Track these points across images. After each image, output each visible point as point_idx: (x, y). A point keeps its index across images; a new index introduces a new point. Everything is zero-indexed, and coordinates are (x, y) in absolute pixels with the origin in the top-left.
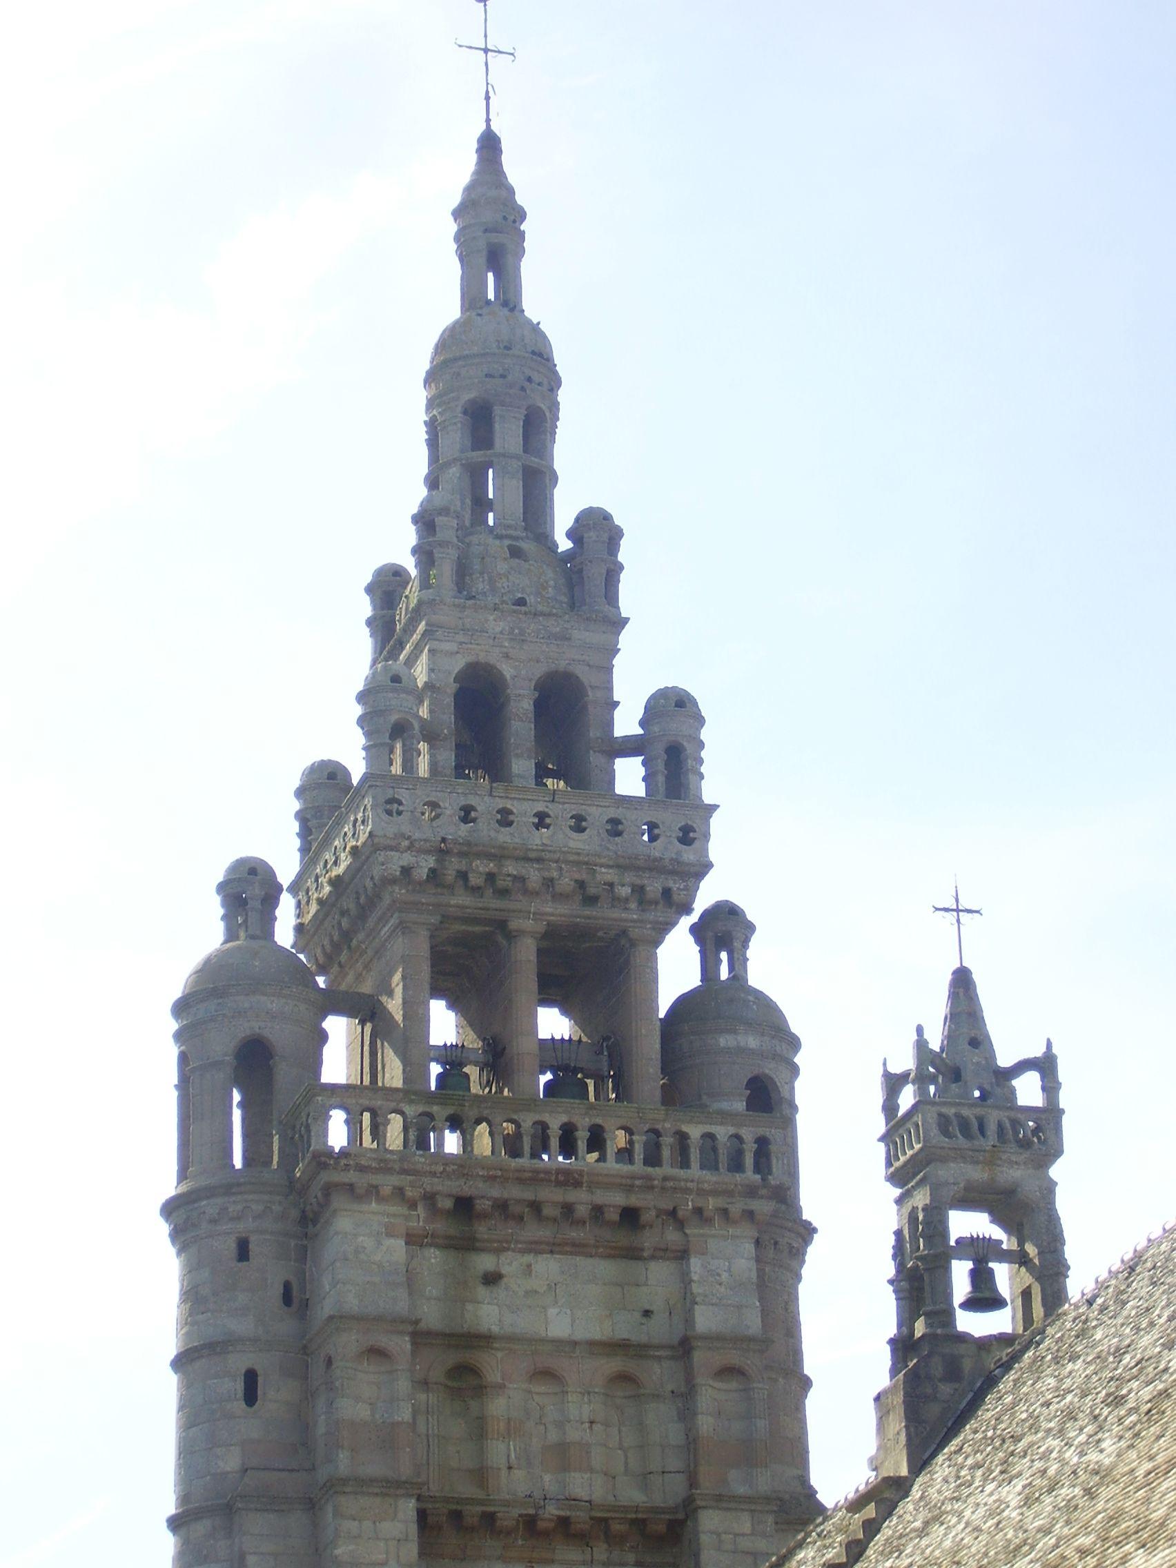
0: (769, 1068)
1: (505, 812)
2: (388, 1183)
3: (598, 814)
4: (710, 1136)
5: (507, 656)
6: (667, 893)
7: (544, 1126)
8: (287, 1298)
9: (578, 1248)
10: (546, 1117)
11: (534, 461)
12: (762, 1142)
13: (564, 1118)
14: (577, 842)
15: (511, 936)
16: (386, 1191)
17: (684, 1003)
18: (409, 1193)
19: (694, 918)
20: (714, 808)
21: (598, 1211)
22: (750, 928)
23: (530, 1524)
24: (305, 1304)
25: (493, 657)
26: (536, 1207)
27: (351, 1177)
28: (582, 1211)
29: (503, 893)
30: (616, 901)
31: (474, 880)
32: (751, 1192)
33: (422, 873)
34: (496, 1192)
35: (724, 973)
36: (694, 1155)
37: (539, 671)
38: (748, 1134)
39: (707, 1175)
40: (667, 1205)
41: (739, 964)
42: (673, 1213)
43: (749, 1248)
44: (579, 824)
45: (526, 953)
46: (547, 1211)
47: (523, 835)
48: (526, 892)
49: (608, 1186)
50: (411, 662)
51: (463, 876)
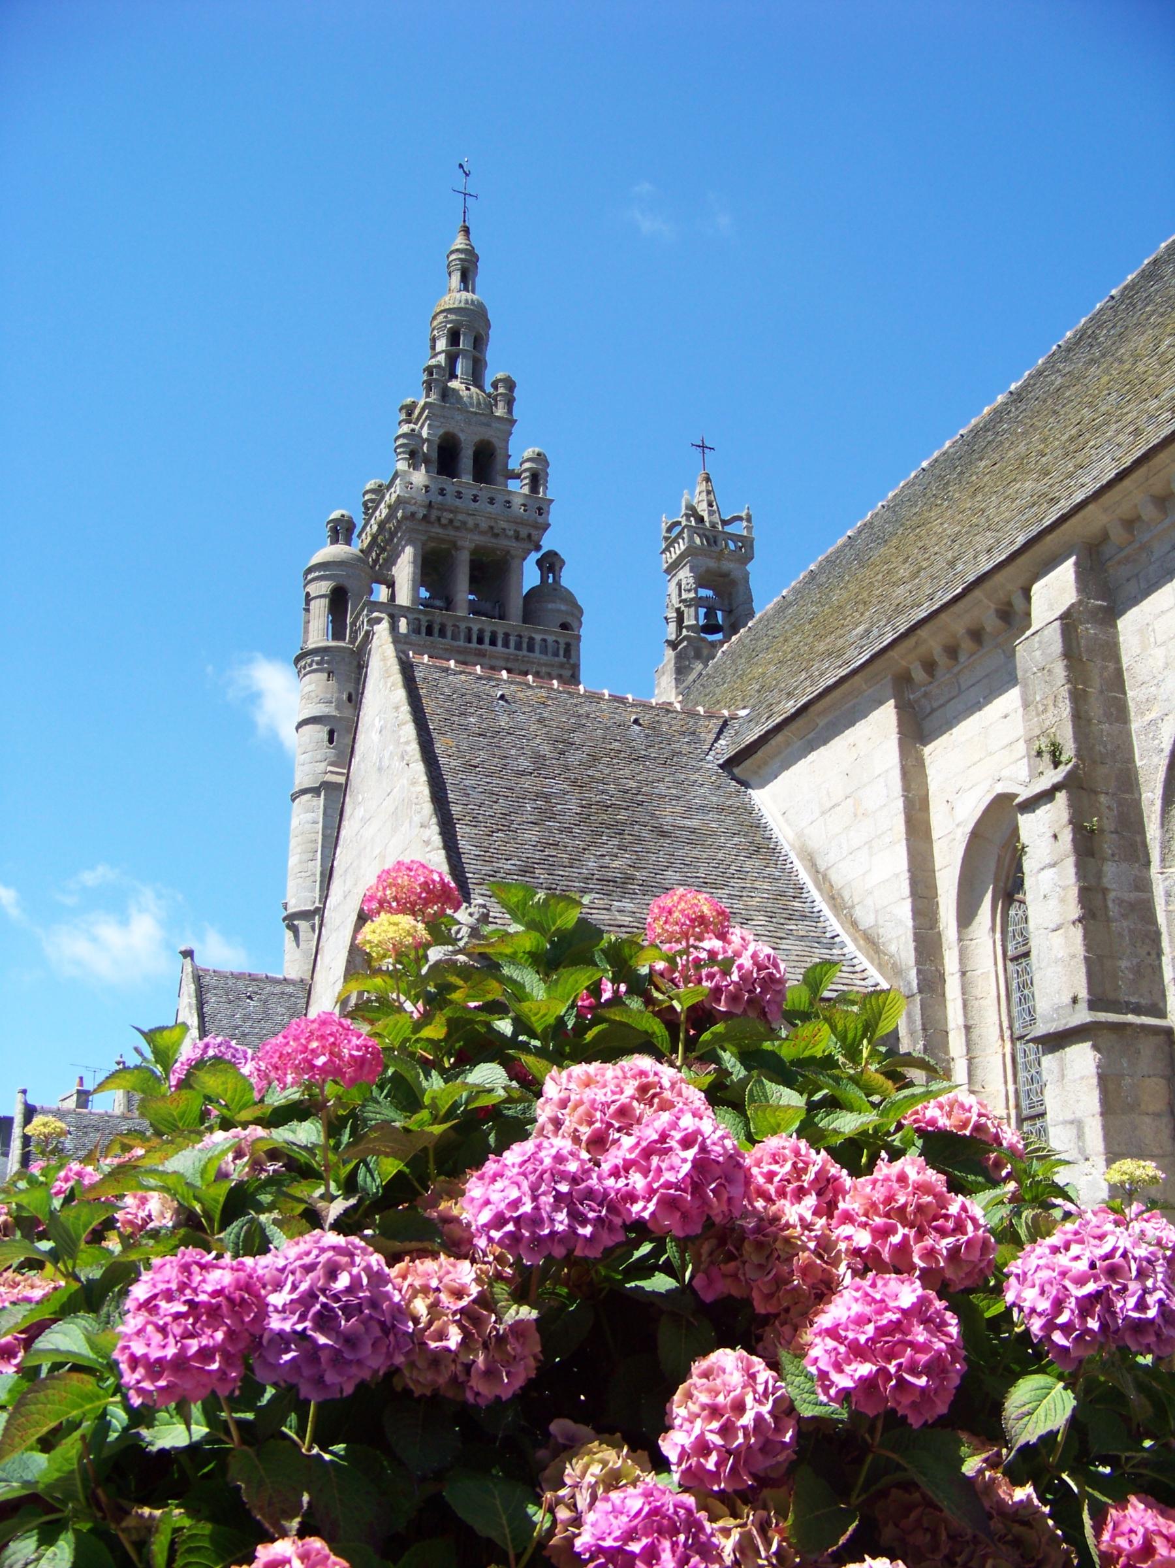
0: (569, 620)
1: (459, 493)
3: (500, 499)
4: (544, 640)
5: (462, 431)
6: (529, 536)
7: (470, 630)
8: (350, 699)
10: (471, 625)
11: (477, 354)
12: (568, 645)
13: (480, 626)
14: (490, 508)
15: (457, 548)
19: (539, 555)
20: (552, 501)
22: (563, 563)
25: (456, 431)
29: (457, 529)
30: (507, 536)
31: (444, 521)
32: (562, 666)
33: (420, 515)
35: (551, 580)
36: (537, 648)
37: (477, 438)
38: (562, 641)
39: (544, 657)
41: (556, 580)
44: (492, 501)
47: (466, 504)
48: (466, 529)
49: (497, 658)
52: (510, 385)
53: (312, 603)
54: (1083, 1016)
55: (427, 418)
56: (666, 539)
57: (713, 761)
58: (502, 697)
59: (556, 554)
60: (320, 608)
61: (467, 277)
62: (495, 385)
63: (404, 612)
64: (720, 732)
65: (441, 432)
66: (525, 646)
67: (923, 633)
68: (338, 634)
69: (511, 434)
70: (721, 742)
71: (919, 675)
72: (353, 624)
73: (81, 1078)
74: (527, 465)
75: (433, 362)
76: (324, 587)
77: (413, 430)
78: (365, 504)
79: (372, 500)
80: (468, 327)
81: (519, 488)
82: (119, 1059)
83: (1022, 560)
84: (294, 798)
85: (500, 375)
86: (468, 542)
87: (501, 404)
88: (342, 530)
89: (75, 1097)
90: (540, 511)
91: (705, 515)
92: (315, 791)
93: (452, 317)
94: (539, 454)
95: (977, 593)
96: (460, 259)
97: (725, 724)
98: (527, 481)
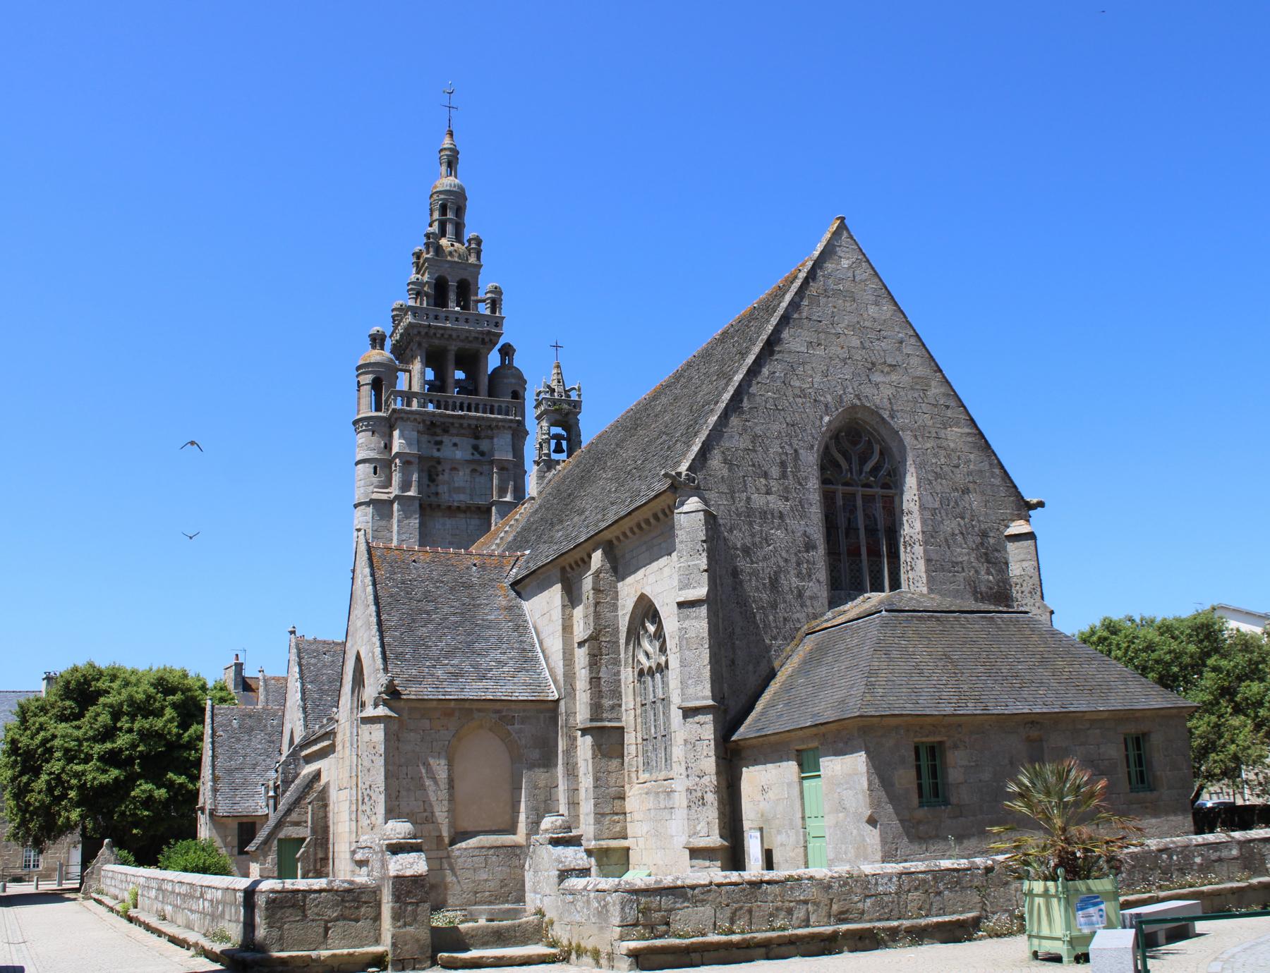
0: (517, 388)
2: (412, 417)
4: (500, 406)
6: (491, 340)
9: (463, 435)
11: (459, 221)
16: (412, 419)
17: (495, 370)
18: (418, 420)
21: (469, 425)
23: (450, 507)
24: (391, 449)
26: (453, 424)
27: (403, 415)
28: (465, 425)
29: (448, 339)
31: (438, 335)
33: (423, 333)
34: (442, 420)
35: (507, 362)
39: (499, 416)
40: (488, 424)
41: (511, 360)
42: (490, 426)
43: (510, 436)
45: (451, 358)
46: (456, 425)
50: (423, 275)
51: (435, 334)
52: (479, 241)
53: (362, 388)
54: (589, 725)
55: (427, 268)
56: (536, 400)
57: (506, 583)
58: (414, 561)
59: (510, 345)
60: (366, 390)
61: (452, 164)
62: (469, 241)
63: (415, 395)
64: (515, 564)
65: (436, 275)
66: (488, 410)
67: (566, 556)
68: (378, 409)
69: (479, 273)
70: (514, 570)
71: (568, 569)
72: (386, 401)
73: (237, 655)
74: (489, 295)
75: (430, 230)
76: (368, 378)
77: (418, 279)
78: (393, 317)
79: (397, 315)
80: (452, 203)
81: (484, 309)
82: (260, 669)
83: (590, 541)
84: (356, 506)
85: (472, 235)
86: (453, 347)
87: (473, 255)
88: (377, 340)
89: (234, 667)
90: (497, 325)
91: (556, 387)
92: (367, 504)
93: (442, 196)
94: (496, 288)
95: (578, 549)
96: (447, 155)
97: (518, 559)
98: (489, 305)
